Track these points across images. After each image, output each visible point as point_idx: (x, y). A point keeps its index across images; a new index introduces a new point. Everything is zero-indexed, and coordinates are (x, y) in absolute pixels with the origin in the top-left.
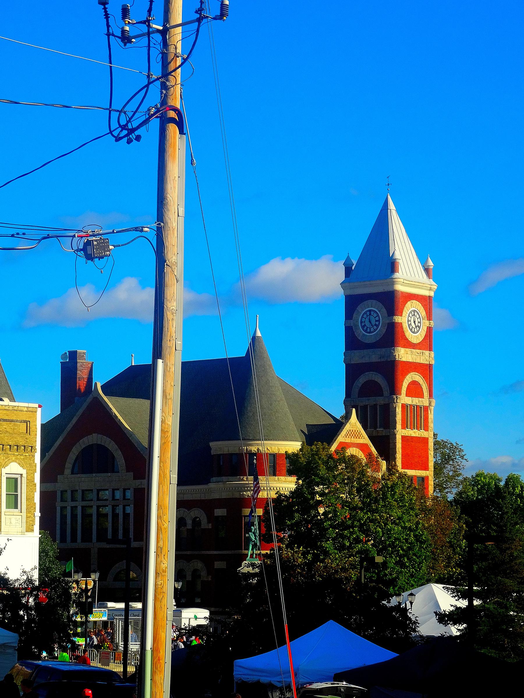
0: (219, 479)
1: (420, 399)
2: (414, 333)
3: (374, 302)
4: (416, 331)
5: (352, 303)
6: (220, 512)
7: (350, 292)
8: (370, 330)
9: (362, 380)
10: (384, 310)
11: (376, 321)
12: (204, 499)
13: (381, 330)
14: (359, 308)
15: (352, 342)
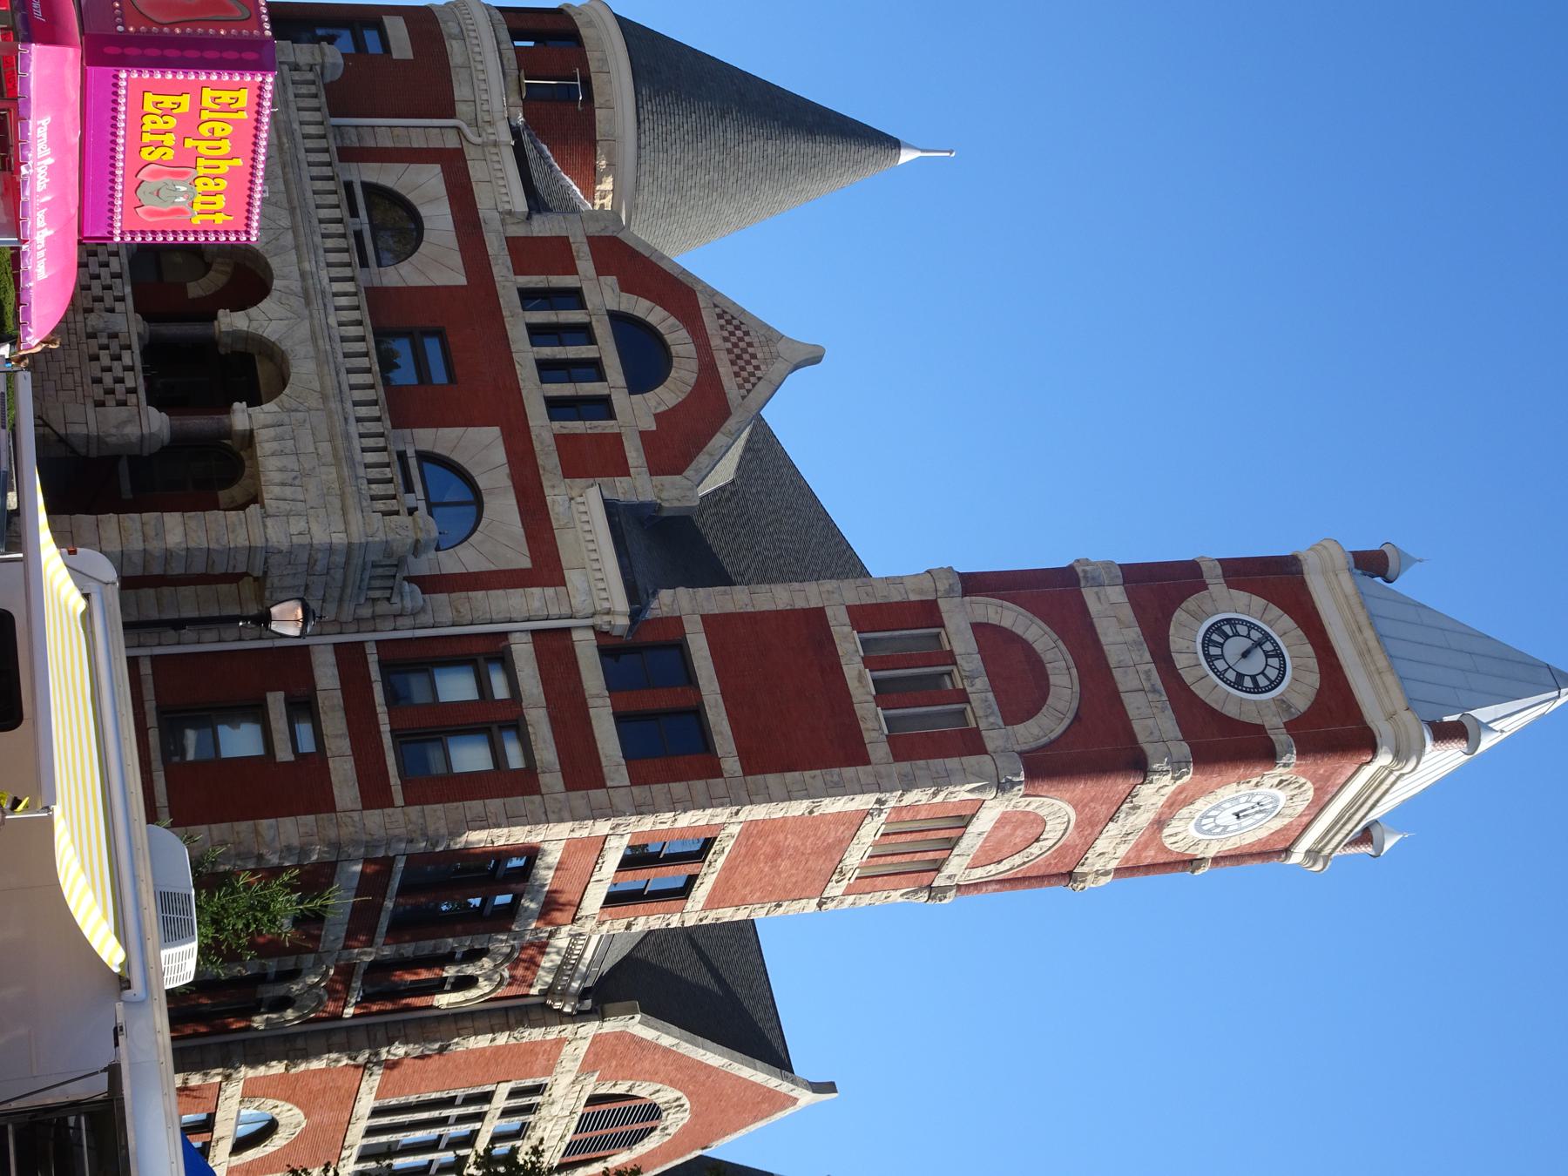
8: (1217, 657)
10: (1302, 704)
11: (1253, 678)
15: (1160, 588)
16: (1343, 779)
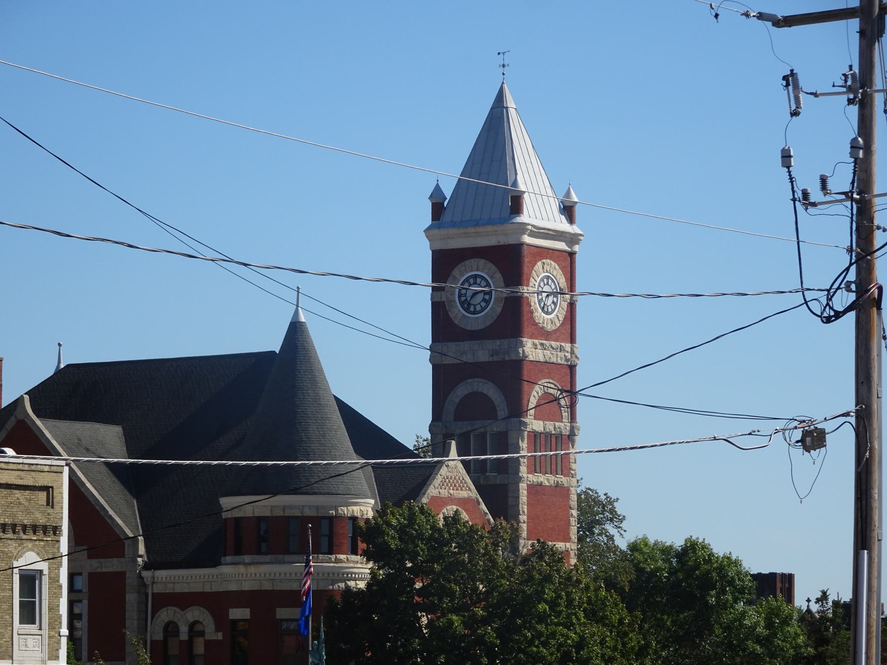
0: (237, 558)
1: (557, 424)
2: (547, 313)
3: (482, 262)
4: (550, 310)
5: (444, 264)
6: (238, 613)
7: (439, 246)
8: (475, 308)
9: (461, 391)
10: (498, 275)
12: (209, 590)
13: (494, 308)
14: (456, 272)
16: (535, 250)
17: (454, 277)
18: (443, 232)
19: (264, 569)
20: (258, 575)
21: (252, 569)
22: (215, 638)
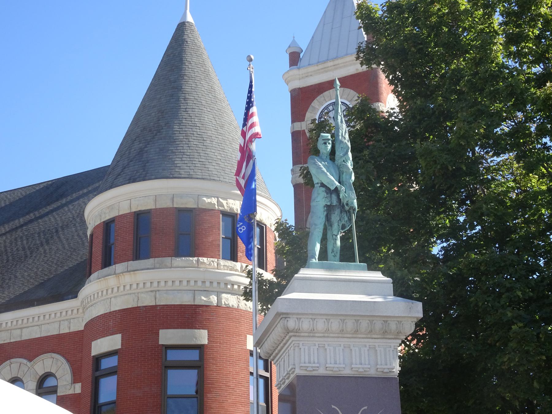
6: (101, 345)
12: (66, 331)
14: (315, 103)
17: (314, 107)
18: (303, 71)
19: (142, 276)
20: (134, 286)
21: (127, 279)
22: (71, 392)
